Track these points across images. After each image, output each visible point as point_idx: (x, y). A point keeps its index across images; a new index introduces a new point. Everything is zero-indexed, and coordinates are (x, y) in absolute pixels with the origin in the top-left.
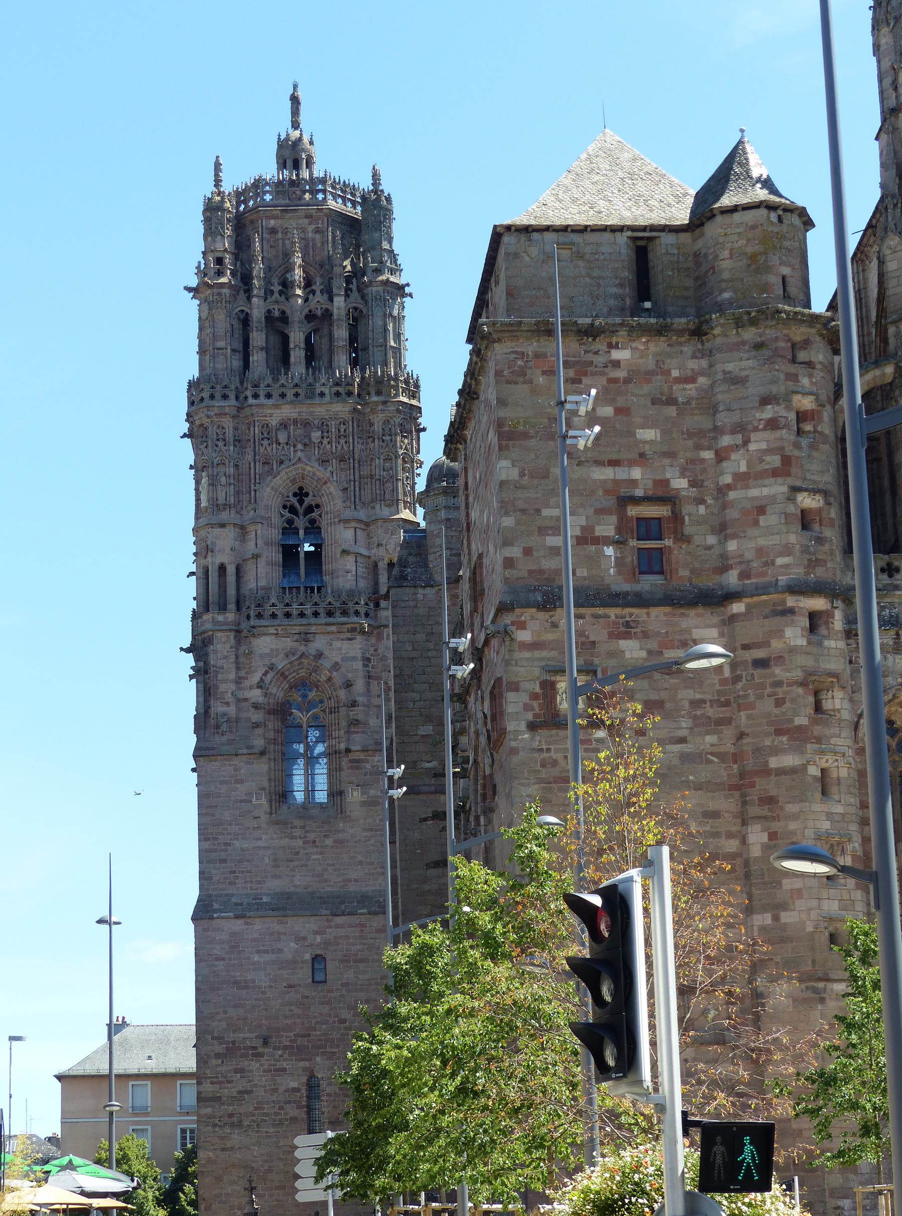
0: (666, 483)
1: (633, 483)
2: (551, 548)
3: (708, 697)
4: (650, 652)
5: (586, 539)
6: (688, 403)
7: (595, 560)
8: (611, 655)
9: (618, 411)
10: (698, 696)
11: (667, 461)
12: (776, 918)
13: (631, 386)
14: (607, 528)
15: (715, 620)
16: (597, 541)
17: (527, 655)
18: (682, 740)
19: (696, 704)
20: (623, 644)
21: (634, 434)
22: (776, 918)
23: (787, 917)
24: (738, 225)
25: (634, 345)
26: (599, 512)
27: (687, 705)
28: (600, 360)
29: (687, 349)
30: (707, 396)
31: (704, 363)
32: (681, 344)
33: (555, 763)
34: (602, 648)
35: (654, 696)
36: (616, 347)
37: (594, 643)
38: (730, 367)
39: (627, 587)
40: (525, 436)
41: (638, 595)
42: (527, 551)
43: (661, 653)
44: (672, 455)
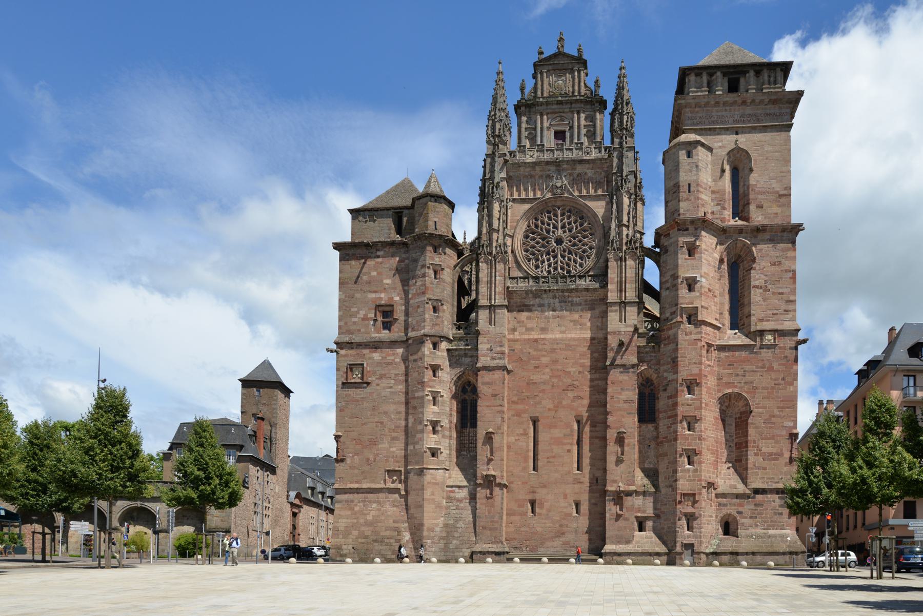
0: (393, 298)
1: (381, 299)
2: (354, 322)
3: (400, 373)
4: (382, 357)
5: (365, 319)
6: (401, 270)
7: (367, 326)
8: (370, 358)
9: (378, 273)
10: (397, 372)
11: (392, 291)
12: (414, 447)
13: (383, 265)
14: (371, 315)
15: (405, 346)
16: (368, 319)
17: (343, 358)
18: (391, 387)
19: (396, 375)
20: (374, 354)
21: (382, 281)
22: (414, 447)
23: (417, 447)
24: (421, 203)
25: (385, 249)
26: (369, 309)
27: (393, 376)
28: (373, 255)
29: (403, 250)
30: (408, 265)
31: (407, 255)
32: (400, 248)
33: (350, 395)
34: (367, 356)
35: (383, 372)
36: (379, 250)
37: (364, 355)
38: (414, 255)
39: (377, 335)
40: (347, 283)
41: (380, 338)
42: (346, 323)
43: (386, 358)
44: (395, 288)
